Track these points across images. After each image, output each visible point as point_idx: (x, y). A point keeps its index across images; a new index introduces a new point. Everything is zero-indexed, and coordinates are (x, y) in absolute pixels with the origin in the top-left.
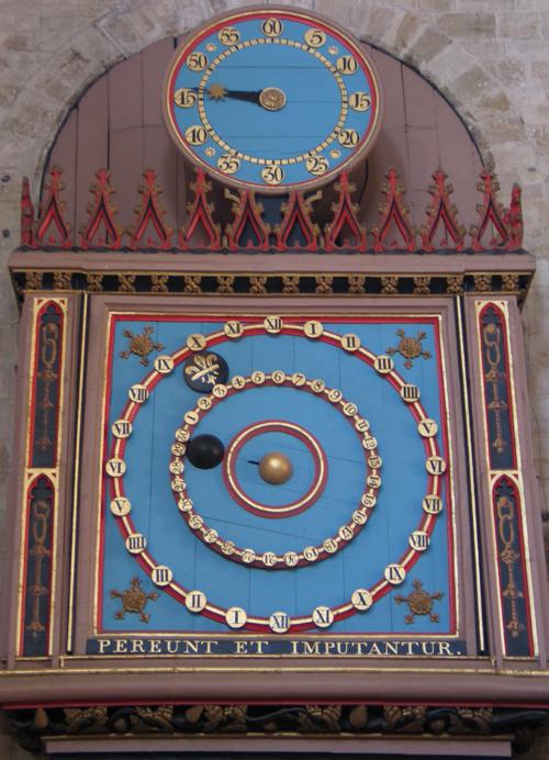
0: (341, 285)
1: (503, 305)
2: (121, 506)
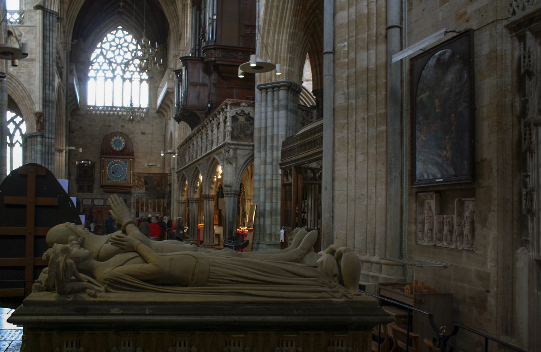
0: (121, 158)
1: (132, 160)
2: (108, 173)
